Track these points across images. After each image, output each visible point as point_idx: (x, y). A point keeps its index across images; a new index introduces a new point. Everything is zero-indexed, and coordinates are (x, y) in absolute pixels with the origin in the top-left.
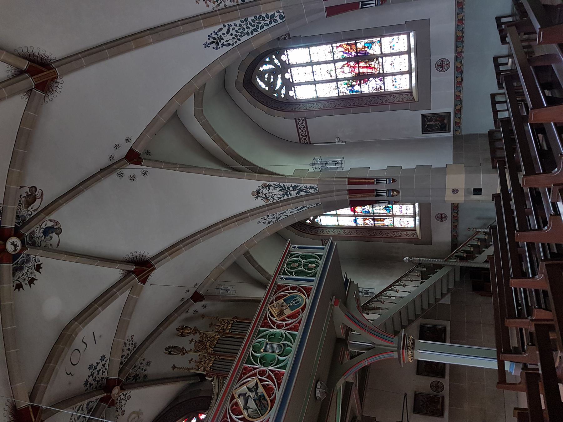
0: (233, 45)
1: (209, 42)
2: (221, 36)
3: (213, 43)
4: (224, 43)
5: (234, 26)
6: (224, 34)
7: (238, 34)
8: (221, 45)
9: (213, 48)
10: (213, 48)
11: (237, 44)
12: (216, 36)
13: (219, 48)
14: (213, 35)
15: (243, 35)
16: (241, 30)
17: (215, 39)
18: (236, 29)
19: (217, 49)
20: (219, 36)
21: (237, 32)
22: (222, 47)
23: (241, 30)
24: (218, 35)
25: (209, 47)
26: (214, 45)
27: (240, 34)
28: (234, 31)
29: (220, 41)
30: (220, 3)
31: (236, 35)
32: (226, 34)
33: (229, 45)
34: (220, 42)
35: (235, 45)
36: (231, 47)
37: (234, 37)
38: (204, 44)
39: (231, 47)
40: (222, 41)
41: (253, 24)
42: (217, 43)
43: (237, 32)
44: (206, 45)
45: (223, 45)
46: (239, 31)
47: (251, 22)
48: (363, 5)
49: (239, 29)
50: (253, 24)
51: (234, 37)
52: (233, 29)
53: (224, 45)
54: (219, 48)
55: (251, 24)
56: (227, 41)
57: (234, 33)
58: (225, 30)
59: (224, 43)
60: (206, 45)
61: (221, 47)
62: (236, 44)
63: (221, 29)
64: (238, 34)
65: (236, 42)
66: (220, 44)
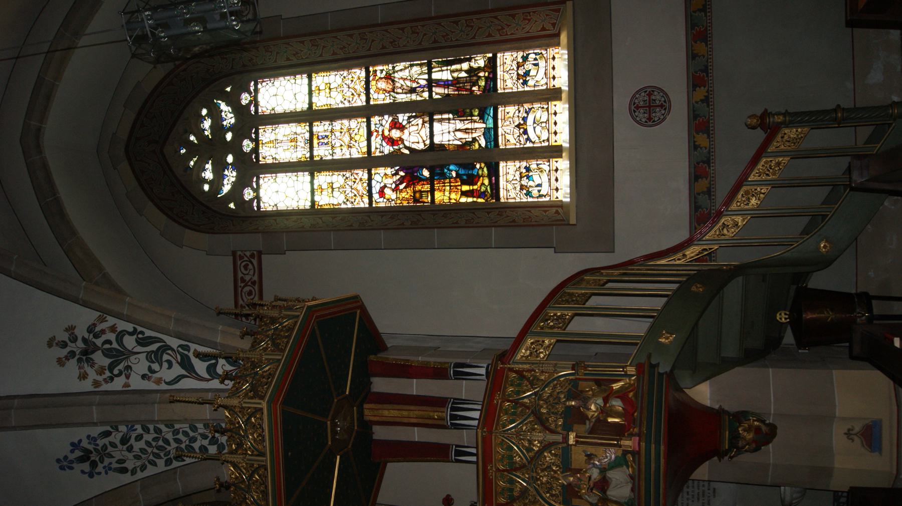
0: (134, 472)
1: (72, 457)
2: (105, 447)
3: (81, 460)
4: (111, 463)
5: (140, 430)
6: (113, 445)
7: (149, 450)
8: (104, 467)
9: (83, 472)
10: (83, 472)
11: (147, 473)
12: (91, 447)
13: (99, 473)
14: (85, 444)
15: (162, 454)
16: (161, 443)
17: (87, 452)
18: (148, 437)
19: (91, 475)
20: (99, 448)
21: (148, 443)
22: (106, 473)
23: (161, 443)
24: (97, 445)
25: (71, 468)
26: (86, 466)
27: (155, 451)
28: (143, 442)
29: (102, 461)
30: (117, 376)
31: (142, 450)
32: (120, 446)
33: (124, 471)
34: (102, 463)
35: (140, 475)
36: (127, 478)
37: (140, 454)
38: (58, 461)
39: (127, 478)
40: (107, 461)
41: (192, 434)
42: (94, 465)
43: (148, 443)
44: (65, 464)
45: (108, 469)
46: (154, 444)
47: (188, 430)
48: (459, 453)
49: (155, 439)
50: (192, 434)
51: (140, 454)
52: (139, 438)
53: (110, 469)
54: (99, 473)
55: (186, 434)
56: (120, 461)
57: (138, 446)
58: (116, 438)
59: (111, 463)
60: (65, 464)
61: (103, 471)
62: (142, 471)
63: (107, 434)
64: (149, 450)
65: (143, 468)
66: (100, 466)
